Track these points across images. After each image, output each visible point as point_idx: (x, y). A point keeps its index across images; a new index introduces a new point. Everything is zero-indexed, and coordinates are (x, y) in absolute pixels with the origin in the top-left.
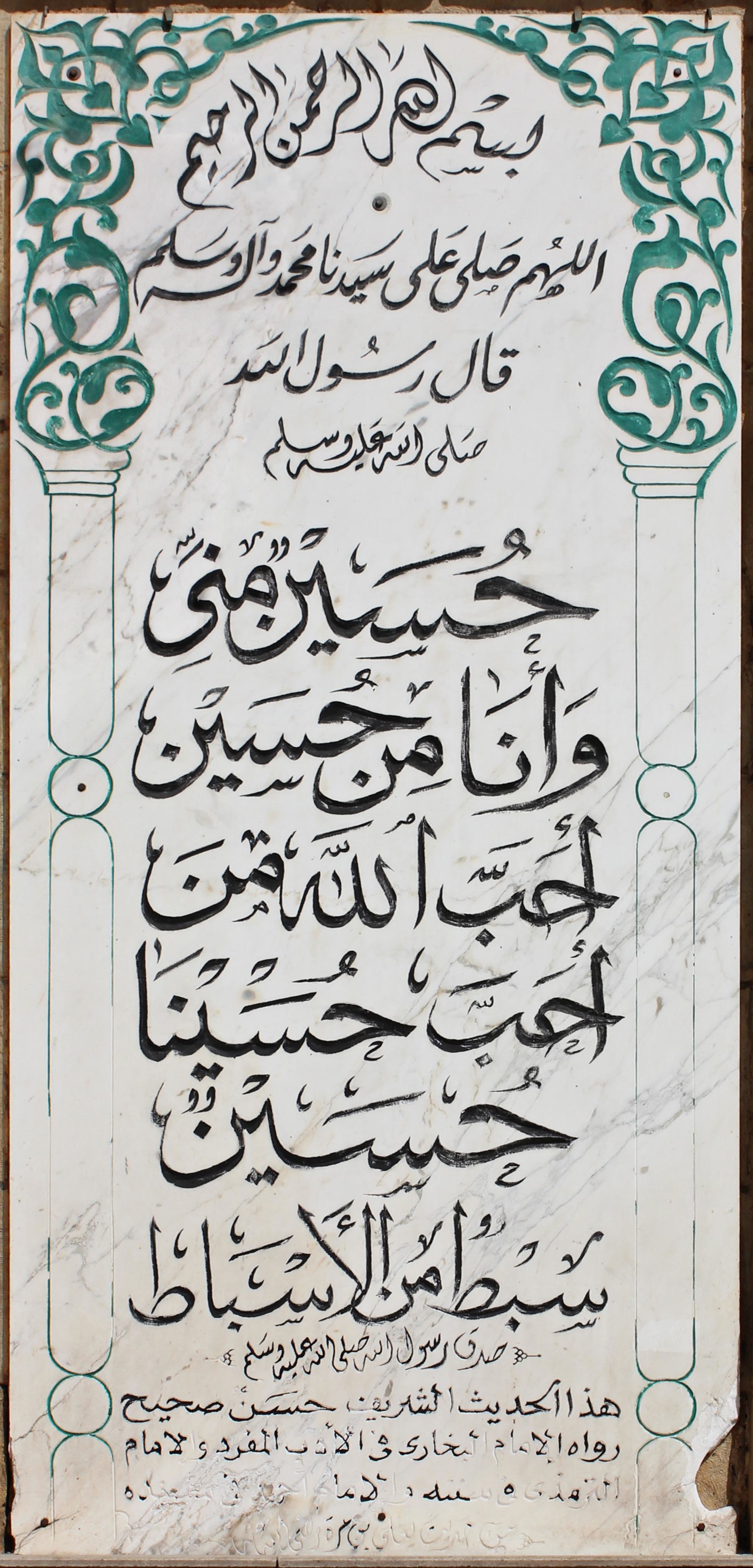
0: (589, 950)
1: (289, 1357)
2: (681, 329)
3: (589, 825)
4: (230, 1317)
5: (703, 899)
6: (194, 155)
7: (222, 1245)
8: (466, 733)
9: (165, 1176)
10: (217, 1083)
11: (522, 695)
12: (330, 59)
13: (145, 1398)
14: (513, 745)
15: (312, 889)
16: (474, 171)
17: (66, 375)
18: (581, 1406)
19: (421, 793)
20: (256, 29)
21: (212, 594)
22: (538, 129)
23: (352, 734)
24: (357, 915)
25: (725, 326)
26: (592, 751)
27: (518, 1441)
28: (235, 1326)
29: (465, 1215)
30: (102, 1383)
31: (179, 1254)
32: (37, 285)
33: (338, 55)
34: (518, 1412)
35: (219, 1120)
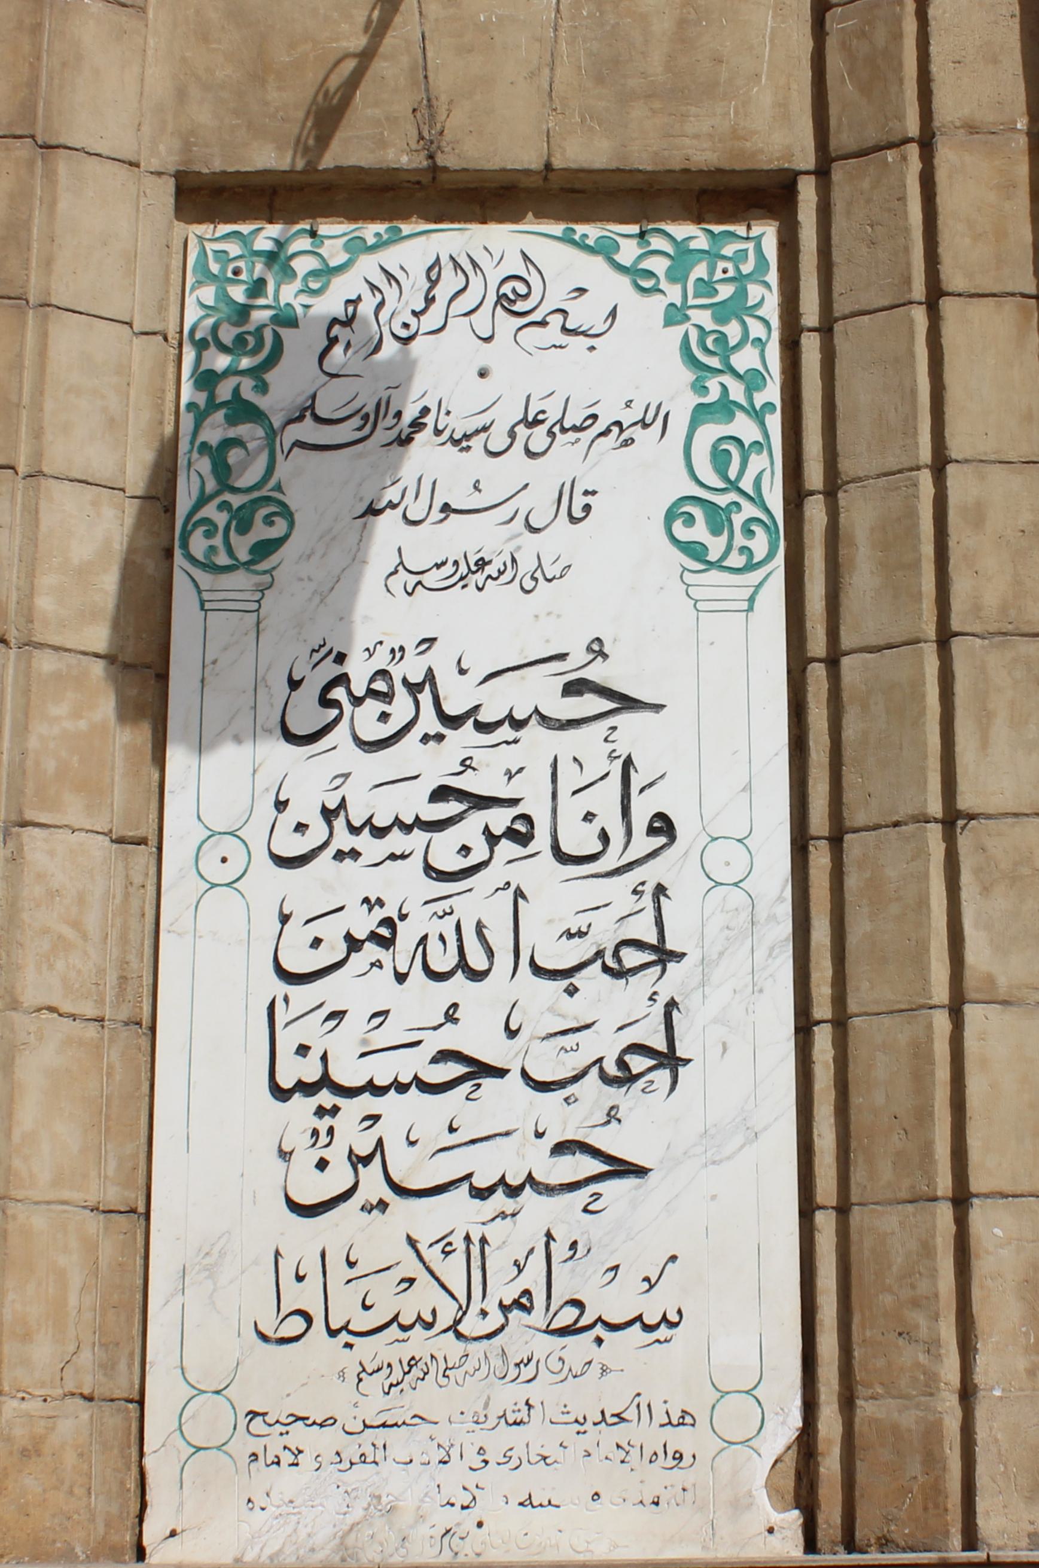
0: (662, 1000)
1: (397, 1374)
2: (732, 474)
3: (660, 890)
4: (344, 1337)
5: (760, 954)
6: (332, 334)
7: (338, 1271)
8: (554, 811)
9: (289, 1207)
10: (336, 1122)
11: (602, 778)
12: (444, 260)
13: (266, 1414)
14: (595, 821)
15: (421, 948)
16: (561, 347)
17: (222, 511)
18: (660, 1417)
19: (516, 863)
20: (385, 237)
21: (339, 693)
22: (613, 314)
23: (457, 812)
24: (460, 971)
25: (769, 471)
26: (663, 826)
27: (603, 1451)
28: (349, 1346)
29: (554, 1240)
30: (228, 1399)
31: (300, 1278)
32: (203, 437)
33: (452, 258)
34: (603, 1424)
35: (337, 1155)
